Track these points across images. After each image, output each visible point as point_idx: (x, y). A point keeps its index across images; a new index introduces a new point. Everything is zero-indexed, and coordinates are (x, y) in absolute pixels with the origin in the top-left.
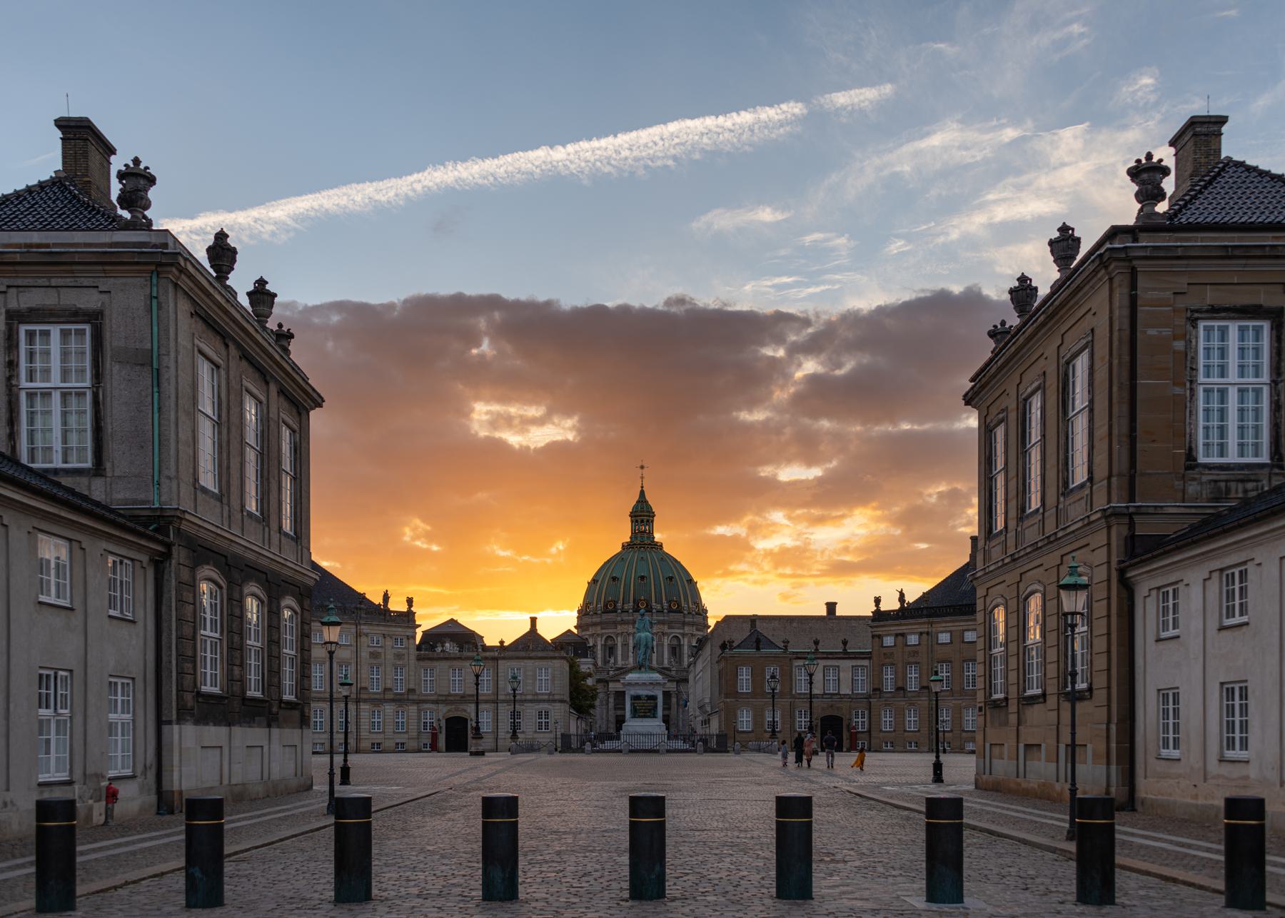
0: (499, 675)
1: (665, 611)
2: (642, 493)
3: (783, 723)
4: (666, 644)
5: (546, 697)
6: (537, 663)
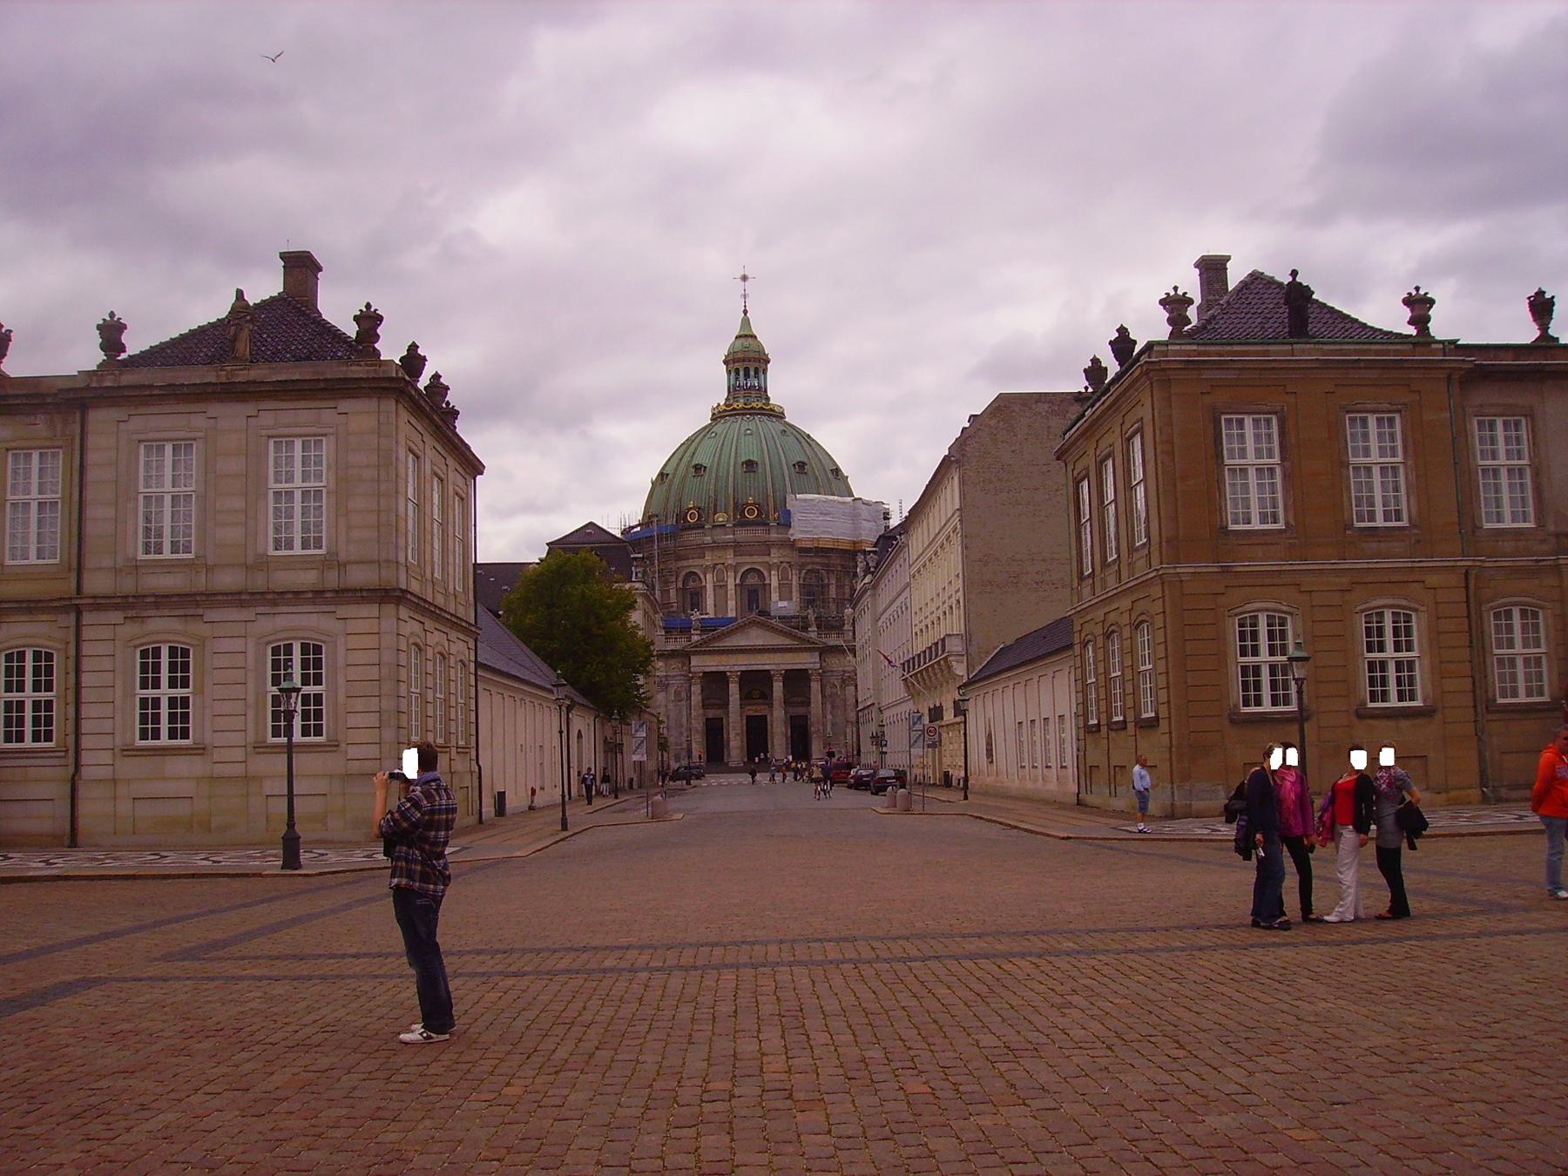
0: (91, 475)
2: (746, 322)
3: (1440, 672)
4: (795, 582)
5: (308, 579)
6: (271, 416)
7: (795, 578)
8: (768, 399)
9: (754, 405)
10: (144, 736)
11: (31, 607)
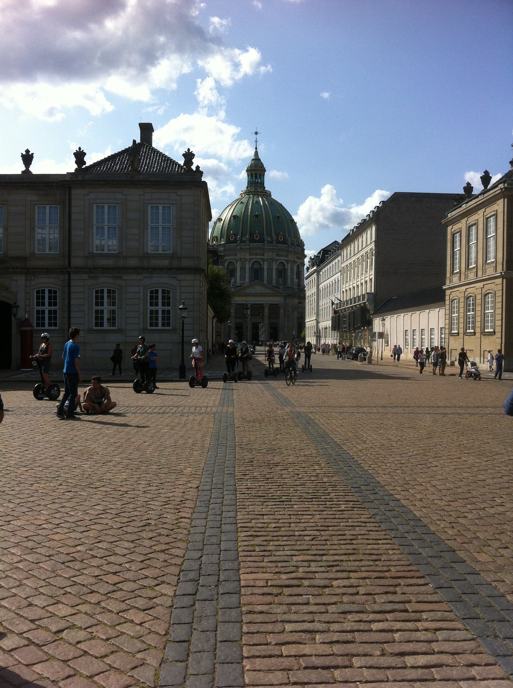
0: (73, 217)
1: (274, 242)
4: (274, 268)
5: (166, 263)
7: (274, 265)
8: (265, 188)
9: (259, 190)
10: (97, 325)
11: (48, 271)
